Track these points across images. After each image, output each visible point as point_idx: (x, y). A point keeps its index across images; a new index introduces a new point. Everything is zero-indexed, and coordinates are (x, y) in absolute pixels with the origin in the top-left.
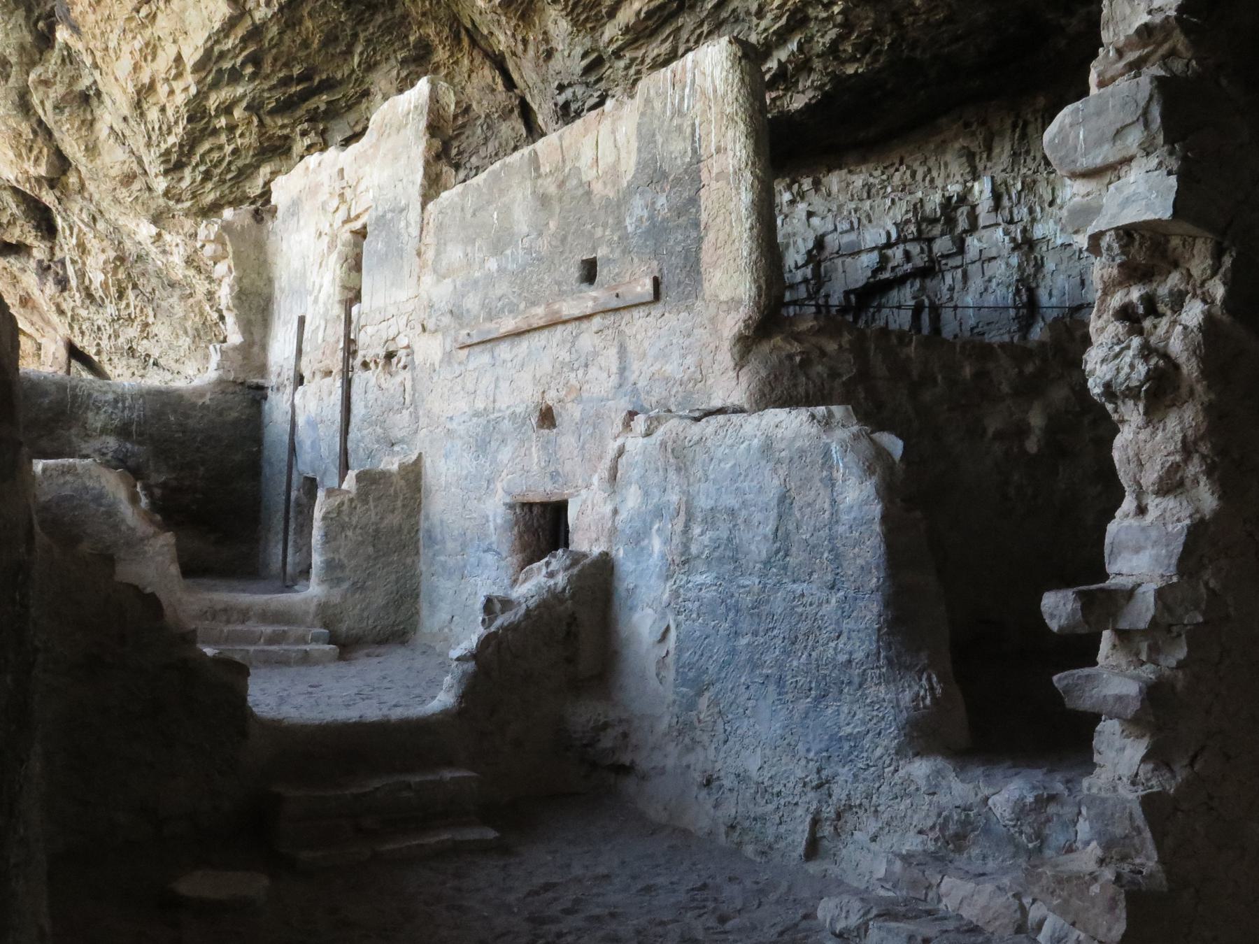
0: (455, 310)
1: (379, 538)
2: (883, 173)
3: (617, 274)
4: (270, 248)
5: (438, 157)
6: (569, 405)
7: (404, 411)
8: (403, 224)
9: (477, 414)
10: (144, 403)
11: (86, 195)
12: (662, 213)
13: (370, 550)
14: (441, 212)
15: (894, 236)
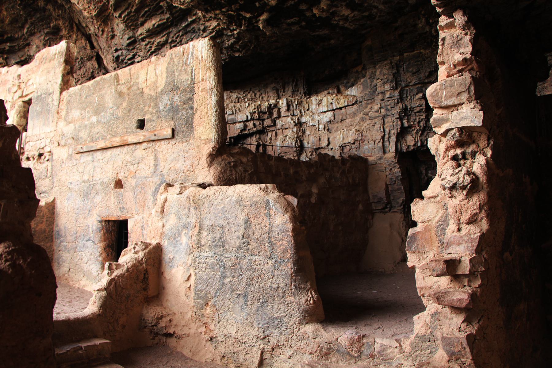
0: (75, 137)
2: (244, 94)
3: (155, 126)
5: (68, 73)
6: (130, 179)
7: (47, 179)
8: (50, 100)
9: (84, 182)
12: (176, 103)
14: (69, 96)
15: (249, 117)
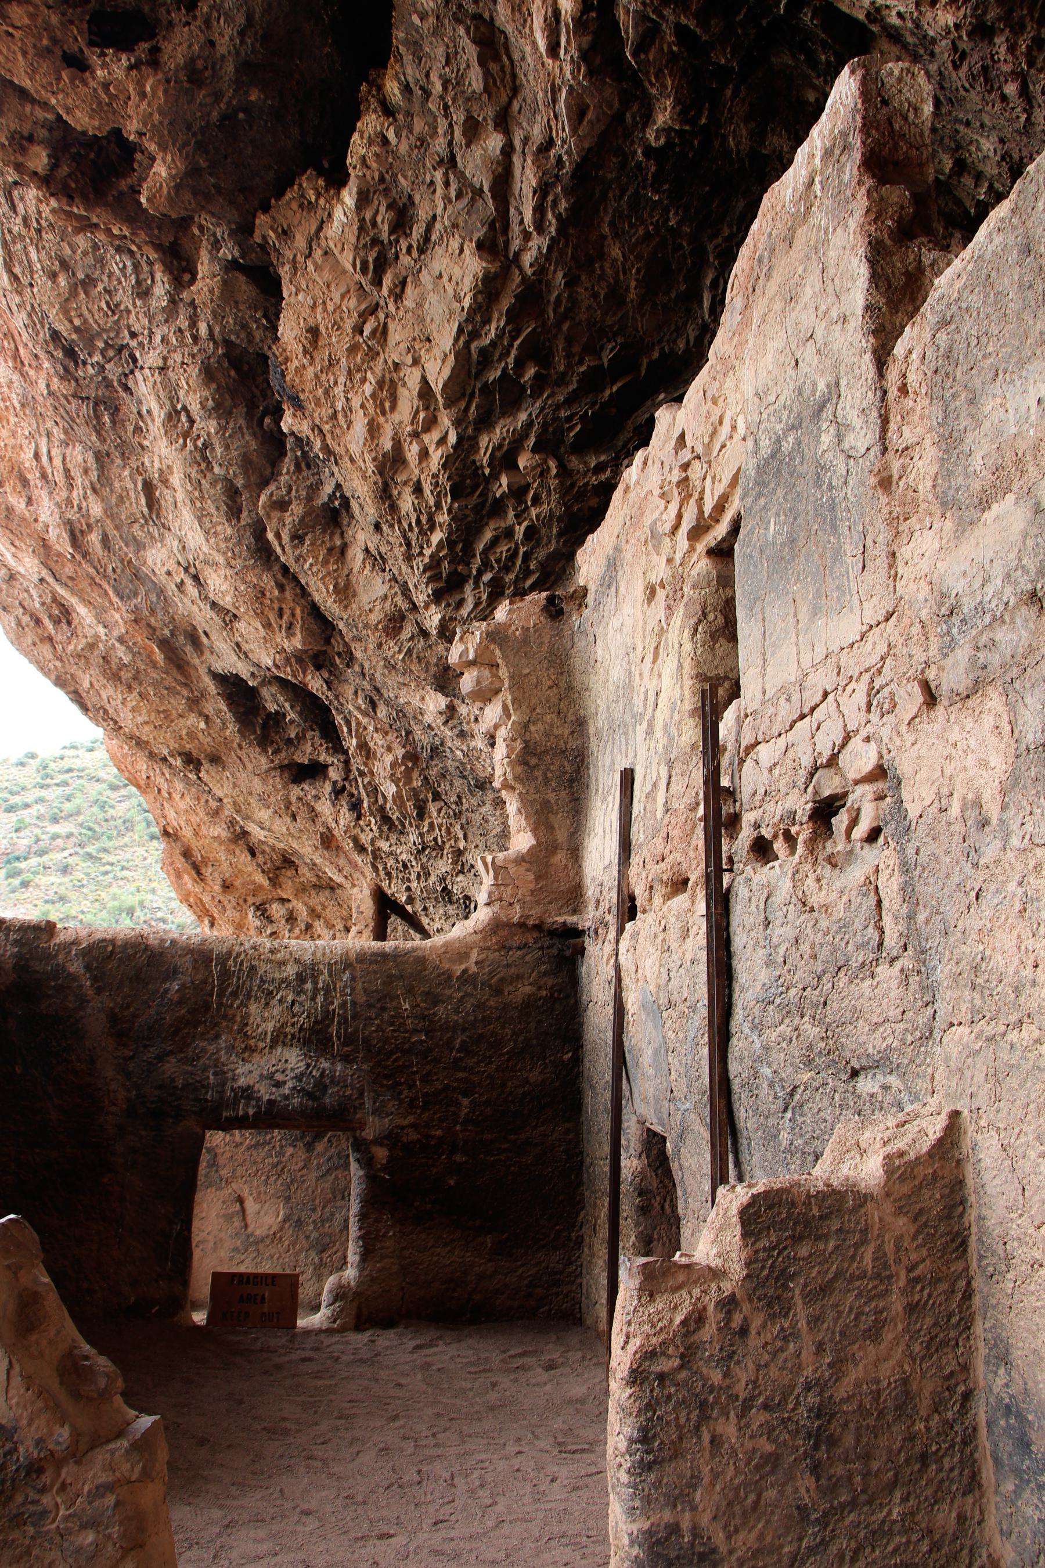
1: (833, 1442)
4: (577, 663)
7: (882, 970)
10: (353, 979)
11: (357, 668)
13: (805, 1483)
